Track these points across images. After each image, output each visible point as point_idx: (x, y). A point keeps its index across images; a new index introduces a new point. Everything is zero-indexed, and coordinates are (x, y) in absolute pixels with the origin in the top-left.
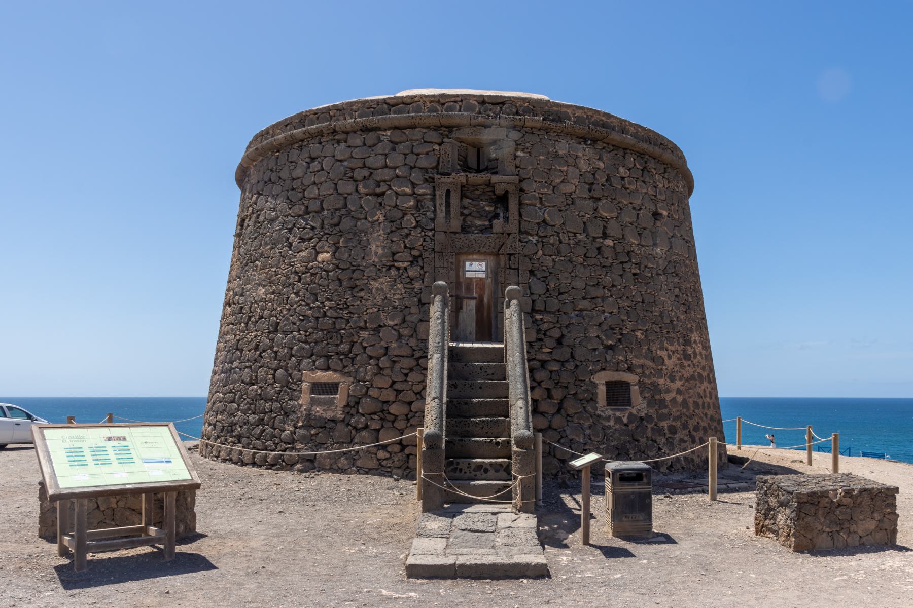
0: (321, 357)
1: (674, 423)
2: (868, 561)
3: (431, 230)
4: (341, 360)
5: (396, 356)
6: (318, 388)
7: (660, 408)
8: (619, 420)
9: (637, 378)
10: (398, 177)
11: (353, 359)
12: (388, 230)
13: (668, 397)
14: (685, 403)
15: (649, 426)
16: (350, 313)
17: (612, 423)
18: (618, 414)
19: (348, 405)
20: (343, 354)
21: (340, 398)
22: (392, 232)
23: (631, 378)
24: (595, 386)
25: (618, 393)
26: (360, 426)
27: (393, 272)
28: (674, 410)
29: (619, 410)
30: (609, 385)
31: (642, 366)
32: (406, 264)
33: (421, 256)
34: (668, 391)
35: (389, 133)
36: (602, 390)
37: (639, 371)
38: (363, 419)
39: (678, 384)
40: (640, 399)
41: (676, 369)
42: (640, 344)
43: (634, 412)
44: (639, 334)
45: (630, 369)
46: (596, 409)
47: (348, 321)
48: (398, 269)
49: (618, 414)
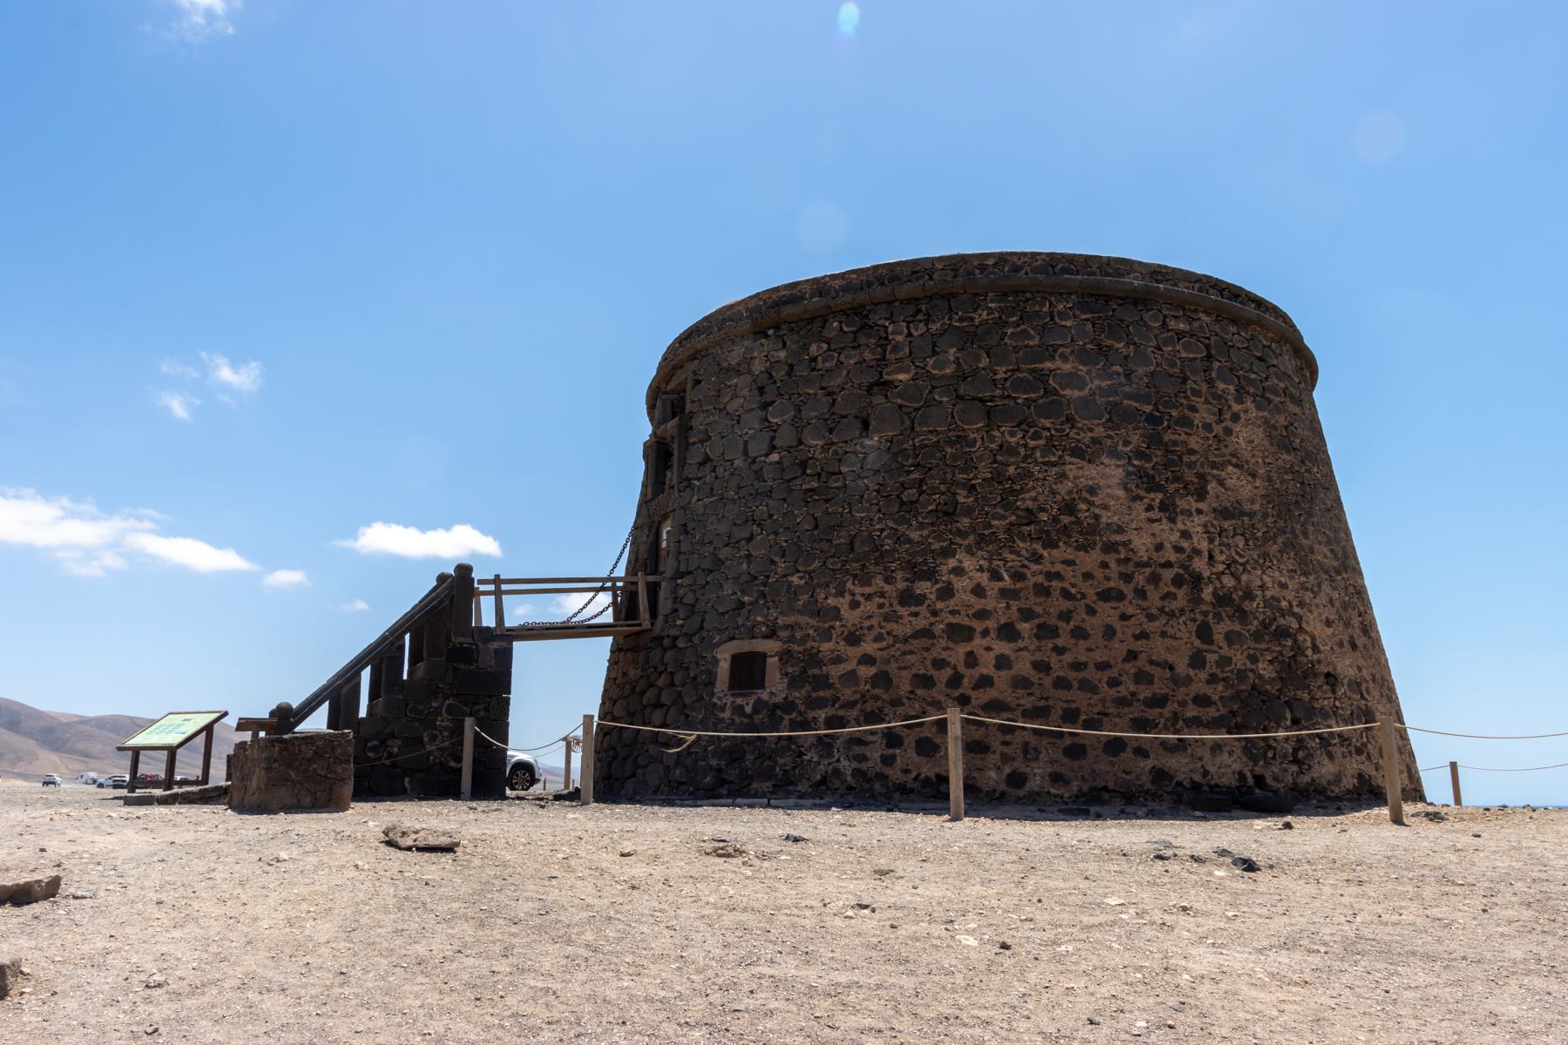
1: (841, 713)
7: (815, 690)
8: (739, 710)
9: (779, 644)
13: (835, 672)
14: (883, 679)
15: (787, 717)
17: (727, 714)
18: (739, 701)
23: (770, 646)
24: (716, 661)
25: (748, 671)
28: (848, 692)
29: (740, 695)
30: (737, 660)
31: (791, 627)
34: (838, 660)
36: (724, 666)
37: (784, 634)
39: (869, 647)
40: (778, 675)
41: (867, 624)
42: (794, 592)
43: (765, 697)
44: (795, 579)
45: (772, 634)
46: (713, 694)
49: (739, 701)
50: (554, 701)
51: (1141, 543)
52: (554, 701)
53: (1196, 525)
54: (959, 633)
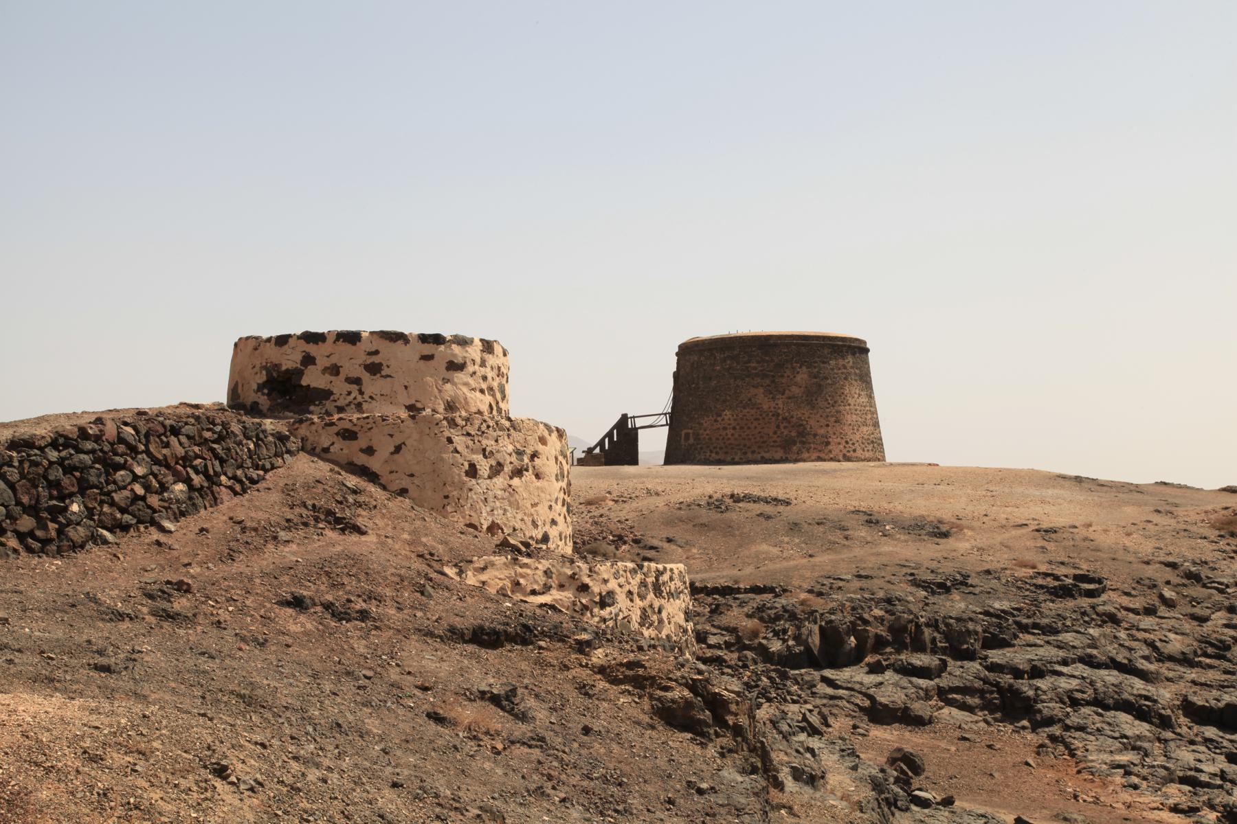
25: (687, 435)
50: (653, 443)
51: (765, 407)
52: (653, 443)
53: (780, 402)
54: (725, 429)
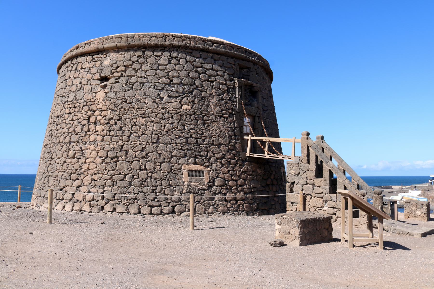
0: (191, 157)
2: (324, 246)
3: (235, 102)
4: (203, 159)
5: (229, 159)
6: (191, 173)
10: (218, 75)
11: (209, 159)
12: (218, 99)
16: (205, 136)
19: (209, 182)
20: (204, 156)
21: (205, 179)
22: (219, 100)
26: (217, 192)
27: (222, 119)
32: (228, 116)
33: (232, 113)
35: (211, 55)
38: (219, 188)
47: (204, 141)
48: (224, 118)
